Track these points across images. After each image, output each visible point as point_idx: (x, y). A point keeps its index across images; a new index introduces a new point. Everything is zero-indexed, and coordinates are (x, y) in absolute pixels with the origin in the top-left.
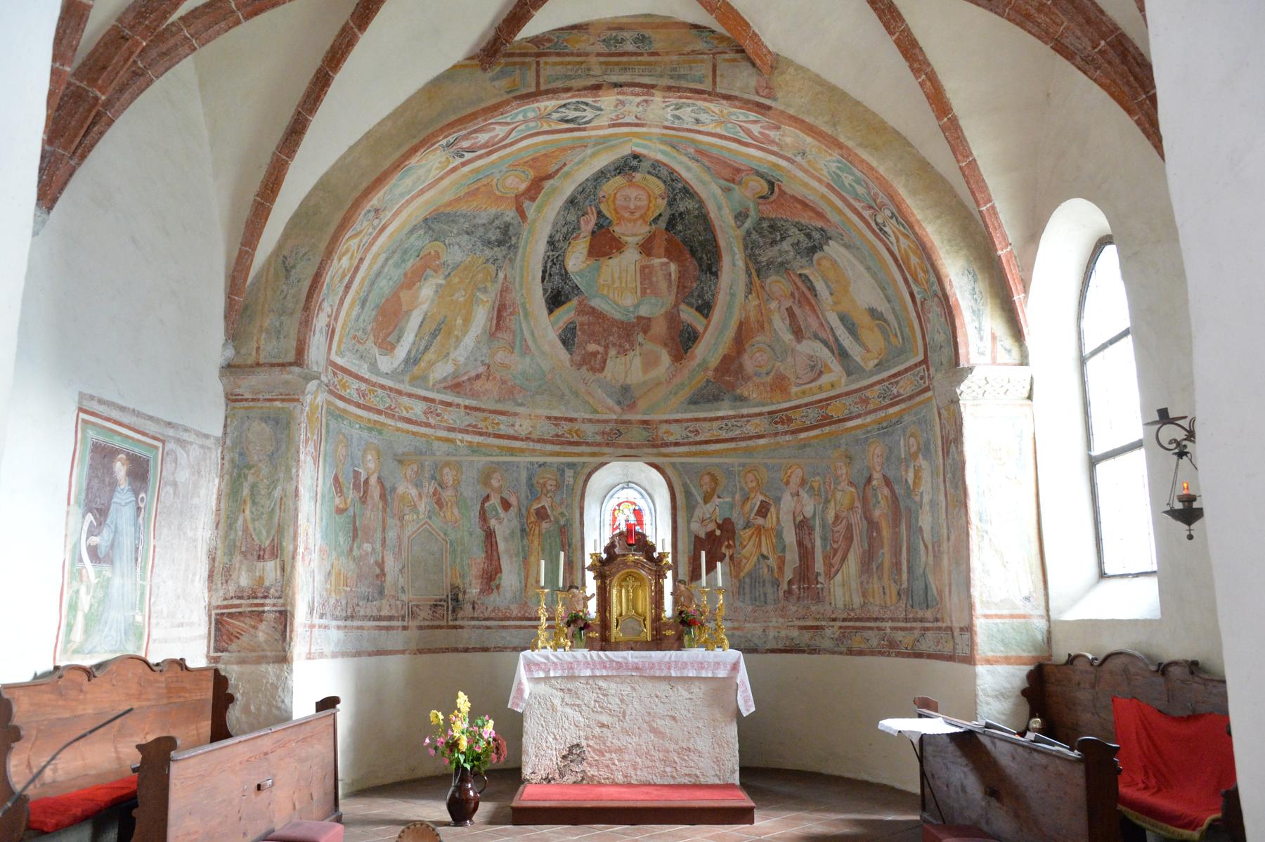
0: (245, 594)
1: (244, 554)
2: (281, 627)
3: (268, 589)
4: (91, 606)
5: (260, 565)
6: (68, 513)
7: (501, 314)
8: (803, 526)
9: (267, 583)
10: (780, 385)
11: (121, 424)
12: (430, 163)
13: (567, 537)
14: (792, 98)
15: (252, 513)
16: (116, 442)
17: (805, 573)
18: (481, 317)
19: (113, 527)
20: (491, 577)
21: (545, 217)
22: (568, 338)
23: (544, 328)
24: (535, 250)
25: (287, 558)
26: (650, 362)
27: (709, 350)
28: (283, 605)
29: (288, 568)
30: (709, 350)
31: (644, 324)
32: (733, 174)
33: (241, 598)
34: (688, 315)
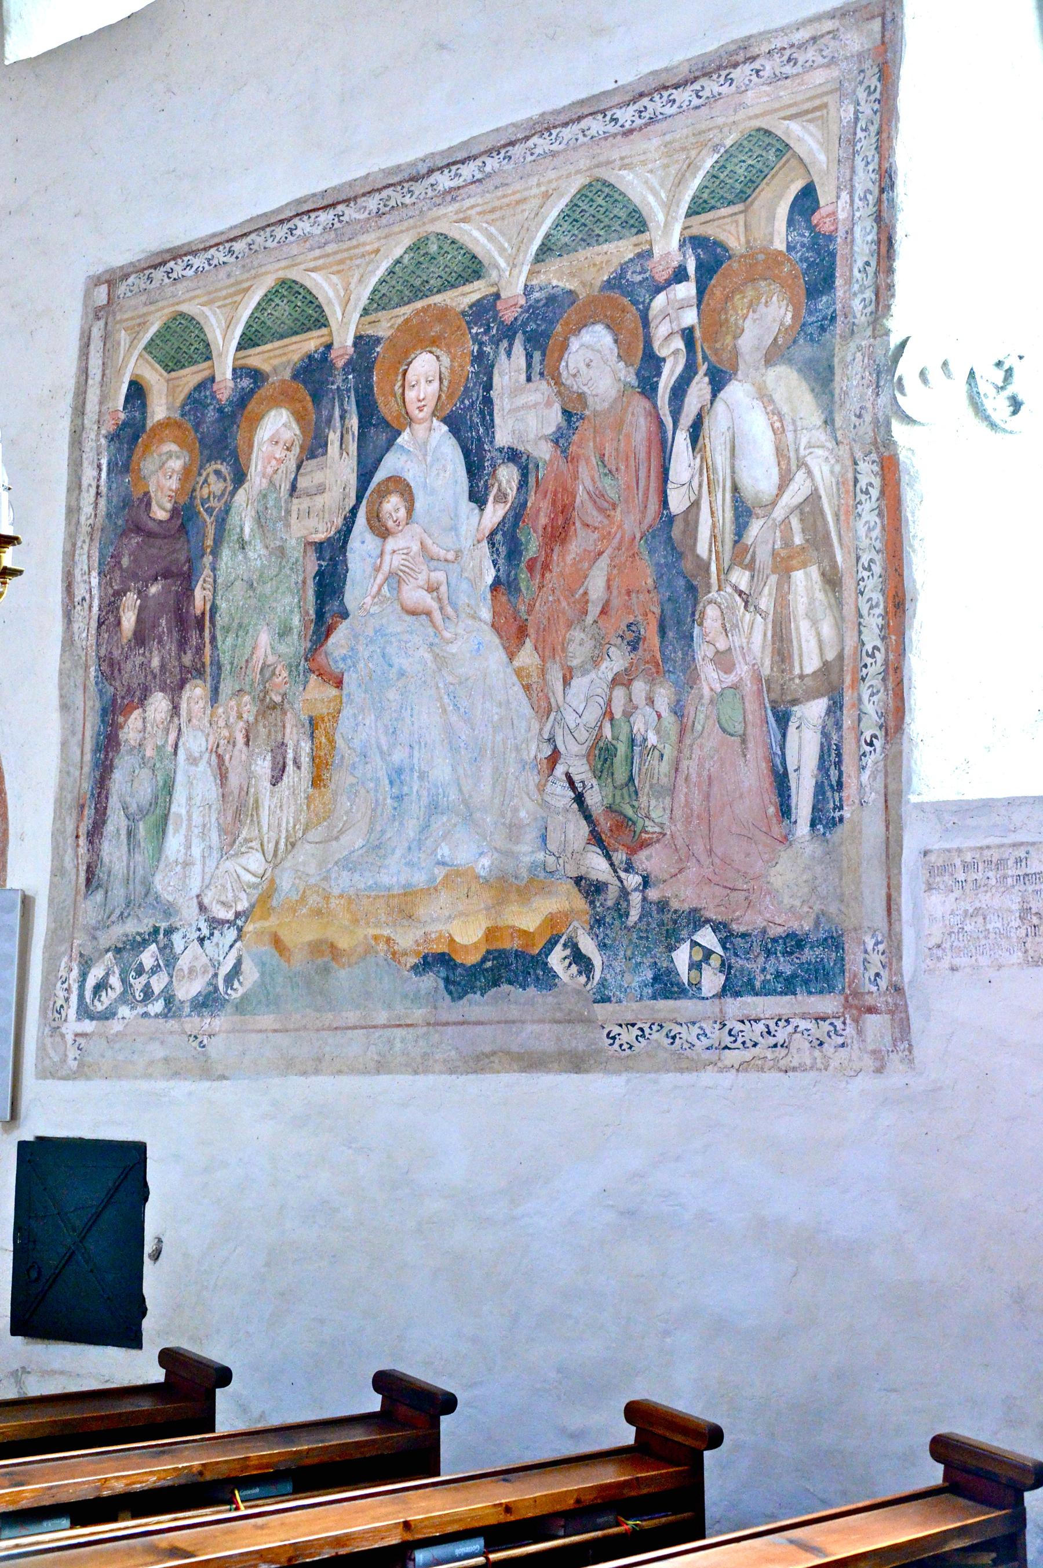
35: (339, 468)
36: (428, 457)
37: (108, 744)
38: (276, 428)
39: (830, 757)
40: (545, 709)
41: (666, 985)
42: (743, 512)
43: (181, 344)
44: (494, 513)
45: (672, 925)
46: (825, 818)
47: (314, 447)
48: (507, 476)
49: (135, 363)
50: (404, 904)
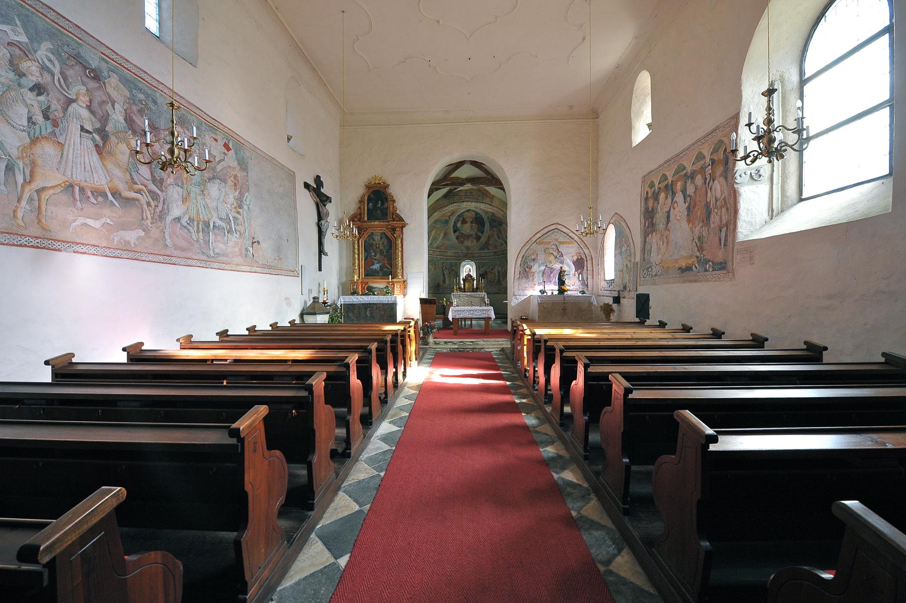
7: (445, 234)
8: (499, 272)
10: (496, 247)
12: (436, 214)
13: (457, 275)
14: (496, 203)
17: (499, 280)
18: (442, 235)
20: (444, 281)
21: (453, 219)
22: (457, 238)
23: (453, 236)
24: (452, 223)
26: (472, 242)
27: (483, 239)
30: (483, 239)
31: (471, 235)
32: (487, 212)
34: (479, 234)
35: (669, 200)
36: (679, 197)
37: (645, 242)
38: (662, 195)
39: (726, 236)
40: (693, 232)
41: (706, 270)
42: (716, 201)
43: (652, 185)
44: (687, 204)
45: (708, 261)
46: (725, 245)
47: (667, 198)
48: (688, 199)
49: (647, 189)
50: (676, 261)
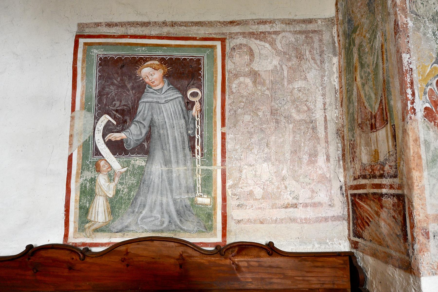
0: (367, 173)
1: (360, 126)
2: (400, 218)
3: (383, 165)
4: (117, 192)
5: (373, 135)
6: (73, 118)
9: (382, 159)
11: (150, 37)
15: (362, 78)
16: (140, 53)
19: (146, 123)
25: (398, 121)
28: (400, 187)
29: (399, 134)
33: (364, 177)
